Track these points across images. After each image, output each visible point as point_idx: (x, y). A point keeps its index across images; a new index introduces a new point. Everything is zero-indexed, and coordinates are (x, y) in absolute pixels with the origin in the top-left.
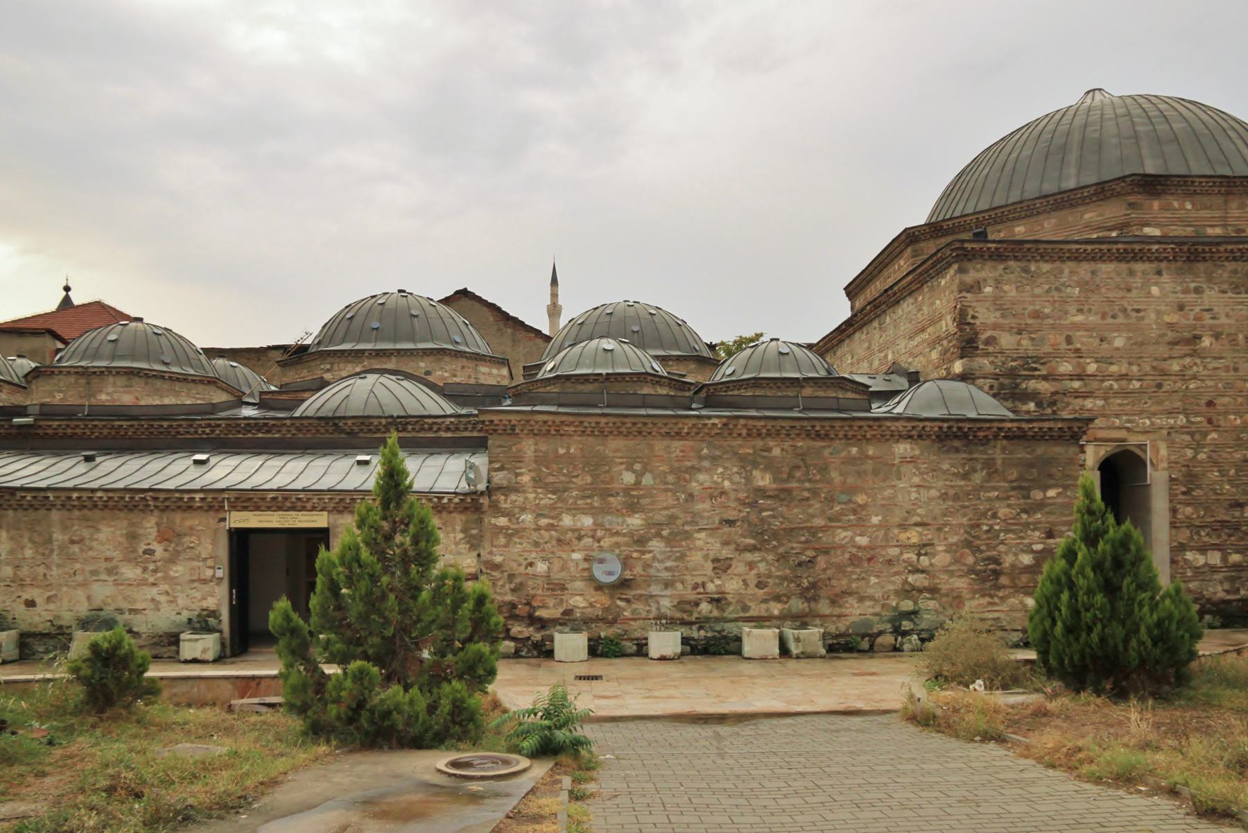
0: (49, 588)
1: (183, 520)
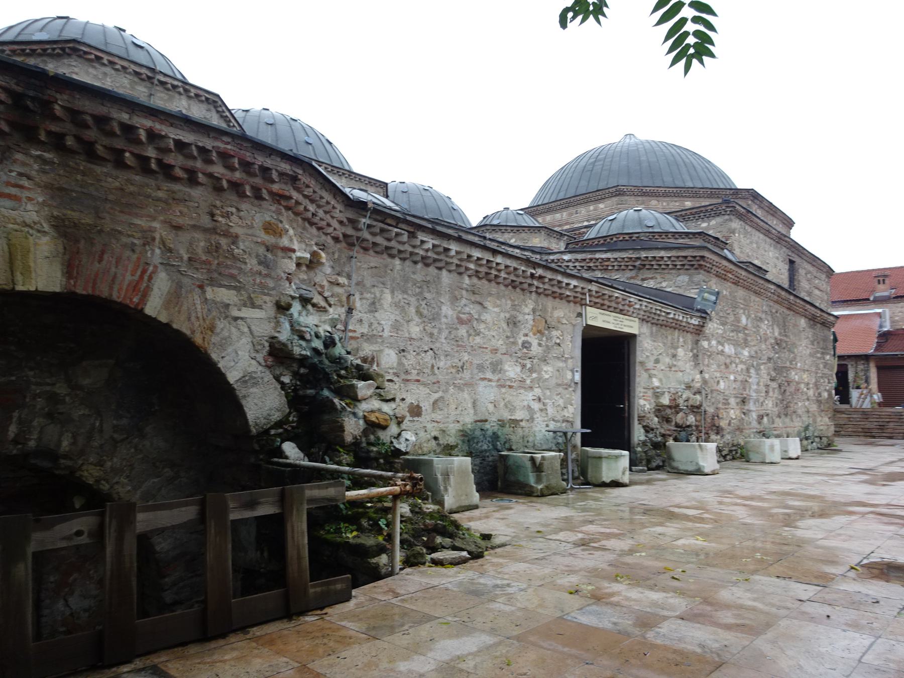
0: (435, 387)
1: (554, 308)
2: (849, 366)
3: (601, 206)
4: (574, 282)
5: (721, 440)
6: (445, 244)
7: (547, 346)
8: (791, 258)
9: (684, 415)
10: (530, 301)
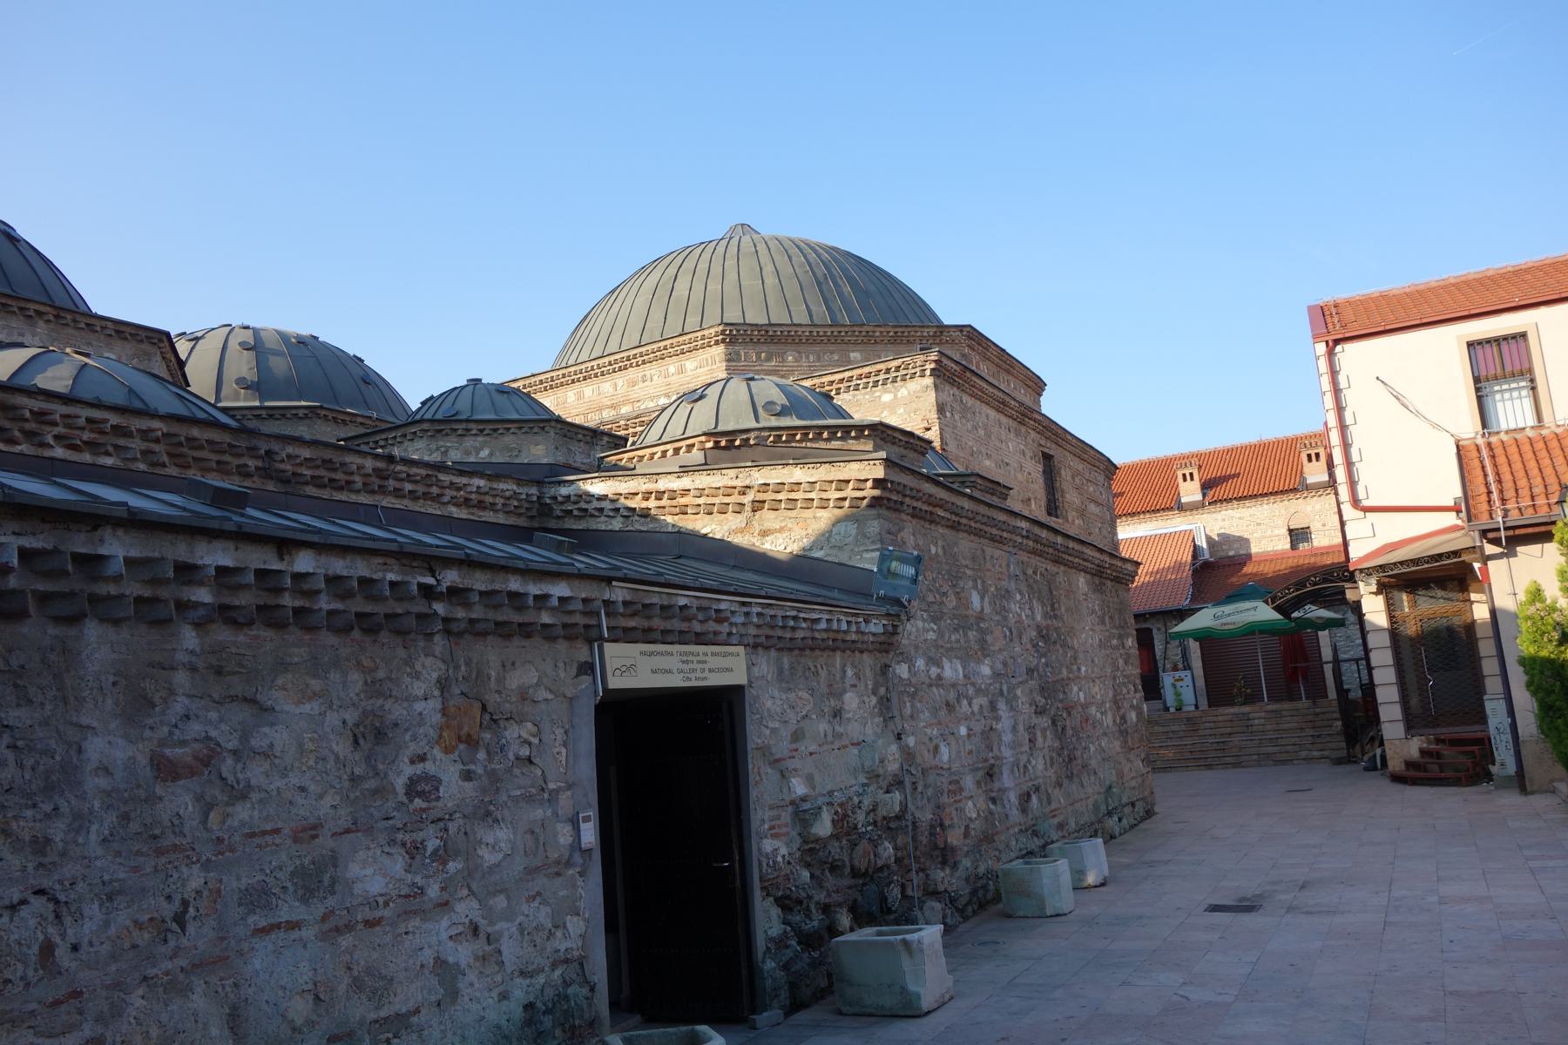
2: (1155, 631)
3: (690, 364)
4: (560, 590)
5: (952, 875)
6: (80, 543)
7: (492, 774)
8: (1046, 450)
9: (870, 848)
10: (429, 661)
